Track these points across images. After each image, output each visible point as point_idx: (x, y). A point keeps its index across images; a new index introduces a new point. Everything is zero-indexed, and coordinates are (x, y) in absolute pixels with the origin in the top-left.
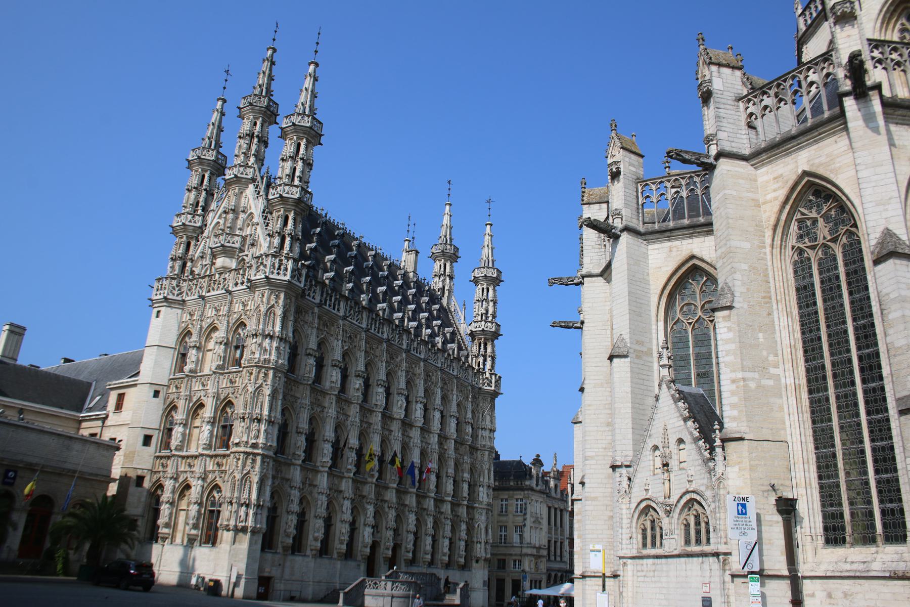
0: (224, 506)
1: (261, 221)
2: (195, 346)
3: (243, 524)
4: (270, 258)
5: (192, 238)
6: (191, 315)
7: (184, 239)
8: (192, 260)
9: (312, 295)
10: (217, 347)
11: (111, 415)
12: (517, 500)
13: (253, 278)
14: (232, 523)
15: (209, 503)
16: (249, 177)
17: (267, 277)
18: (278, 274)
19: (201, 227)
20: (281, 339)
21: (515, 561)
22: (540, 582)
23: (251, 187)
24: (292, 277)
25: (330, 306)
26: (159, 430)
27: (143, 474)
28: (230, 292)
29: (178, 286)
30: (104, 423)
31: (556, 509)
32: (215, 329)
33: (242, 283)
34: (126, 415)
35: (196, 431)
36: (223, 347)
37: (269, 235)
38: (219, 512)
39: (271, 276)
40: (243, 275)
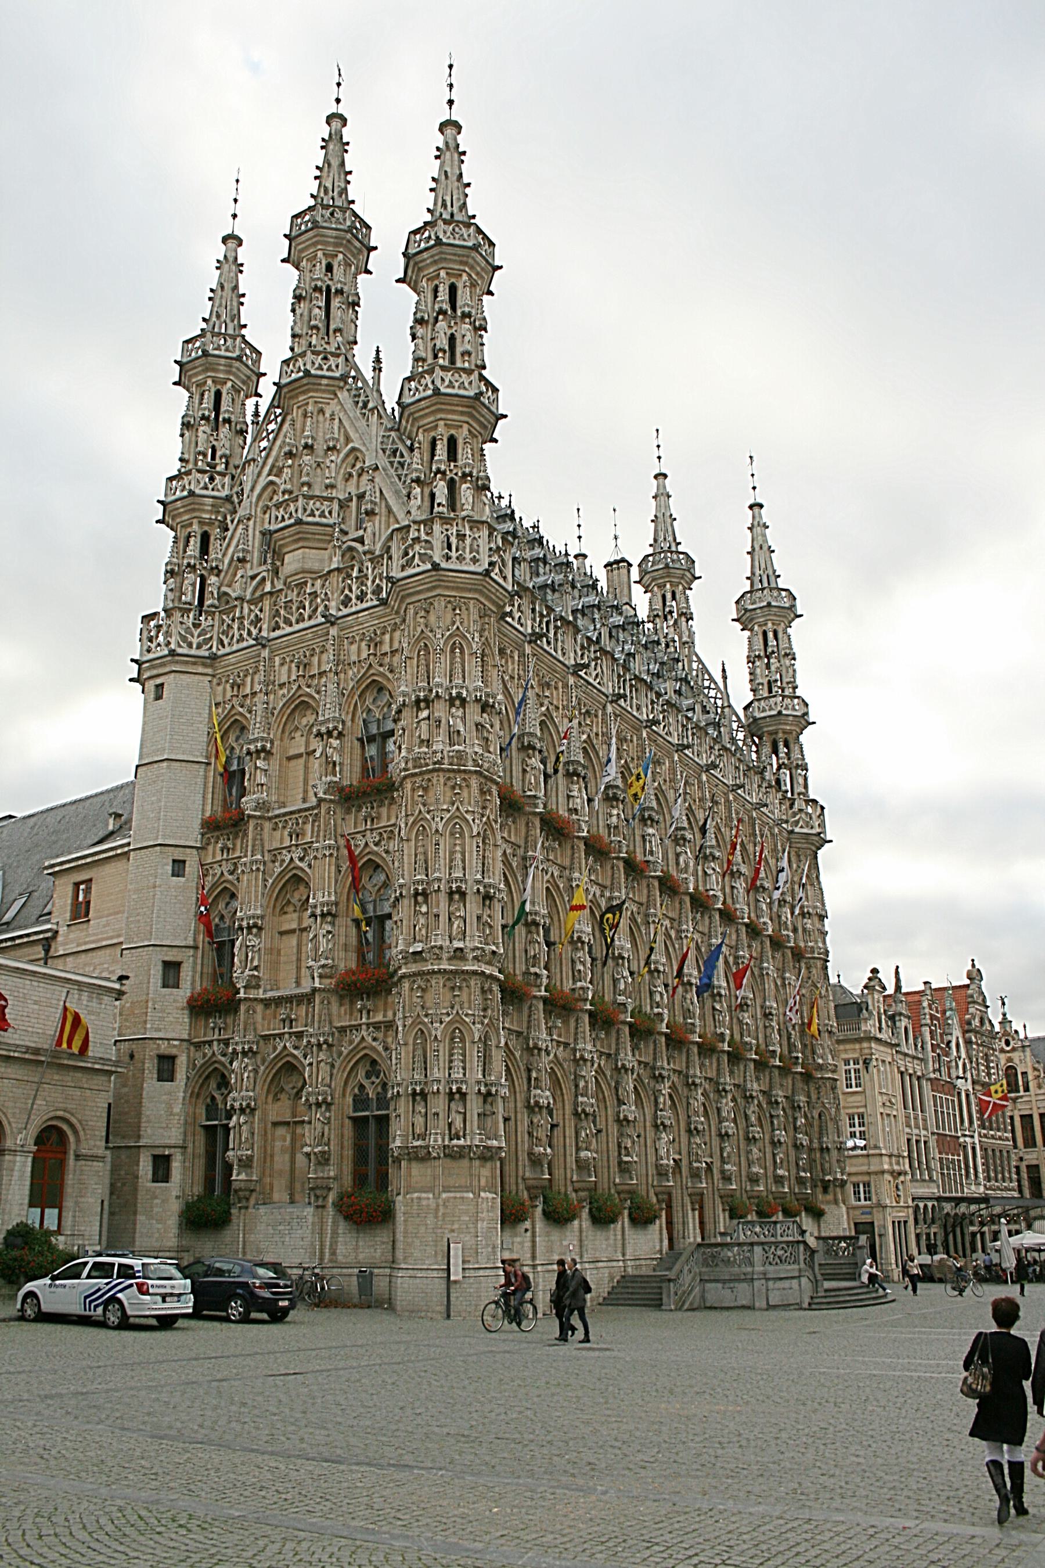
0: (403, 1106)
1: (383, 462)
2: (263, 749)
3: (462, 1142)
4: (437, 527)
5: (211, 523)
6: (237, 686)
7: (195, 527)
8: (216, 571)
9: (517, 615)
10: (317, 745)
11: (62, 930)
12: (847, 1062)
13: (396, 574)
14: (436, 1140)
15: (349, 1100)
16: (337, 374)
17: (436, 567)
18: (460, 559)
19: (228, 499)
20: (485, 707)
21: (856, 1185)
22: (905, 1222)
23: (343, 395)
24: (491, 564)
25: (549, 643)
26: (196, 948)
27: (174, 1051)
28: (331, 621)
29: (196, 626)
30: (47, 951)
31: (910, 1075)
32: (302, 705)
33: (361, 598)
34: (100, 927)
35: (293, 940)
36: (335, 743)
37: (417, 481)
38: (383, 1122)
39: (444, 565)
40: (362, 578)
